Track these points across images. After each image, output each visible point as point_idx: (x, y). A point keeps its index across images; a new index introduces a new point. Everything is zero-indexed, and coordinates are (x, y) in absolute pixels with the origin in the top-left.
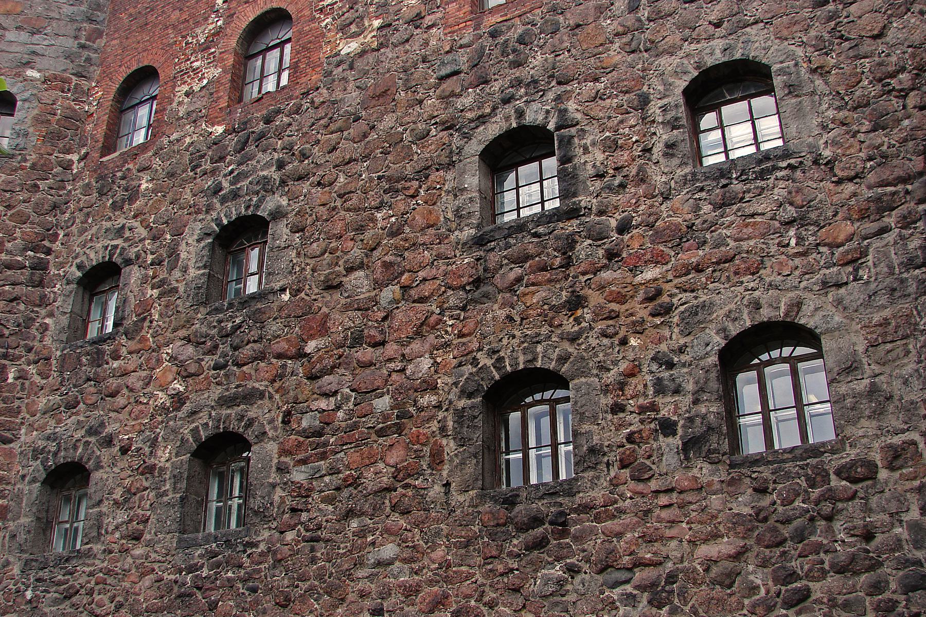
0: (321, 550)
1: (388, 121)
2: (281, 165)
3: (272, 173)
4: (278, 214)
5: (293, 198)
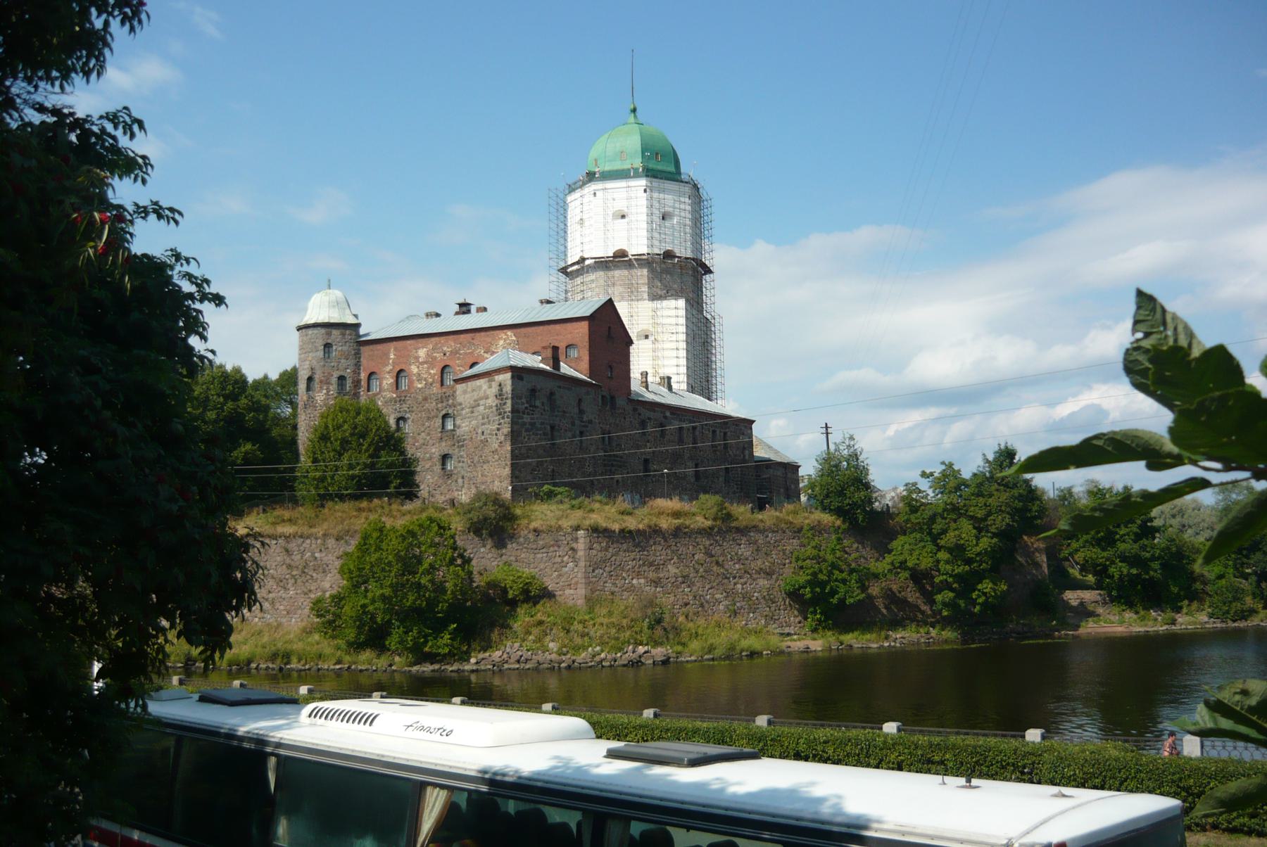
4: (409, 418)
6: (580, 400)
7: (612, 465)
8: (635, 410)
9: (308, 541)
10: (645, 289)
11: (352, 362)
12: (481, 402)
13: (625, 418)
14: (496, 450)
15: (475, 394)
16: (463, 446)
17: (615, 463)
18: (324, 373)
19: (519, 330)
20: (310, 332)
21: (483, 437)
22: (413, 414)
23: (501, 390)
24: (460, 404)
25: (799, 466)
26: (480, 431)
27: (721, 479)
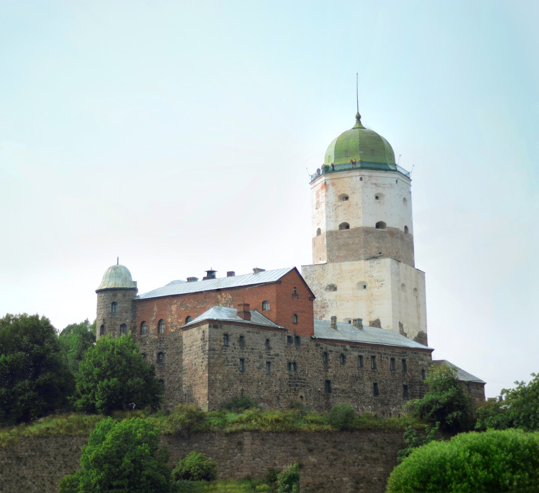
0: (172, 394)
1: (177, 344)
2: (165, 346)
3: (164, 347)
4: (165, 353)
5: (167, 351)
6: (268, 341)
7: (297, 385)
8: (317, 345)
9: (75, 439)
10: (361, 251)
11: (129, 315)
12: (195, 343)
13: (308, 352)
15: (192, 337)
16: (185, 373)
17: (299, 384)
18: (111, 323)
19: (234, 291)
22: (168, 350)
23: (204, 336)
25: (484, 384)
27: (399, 394)
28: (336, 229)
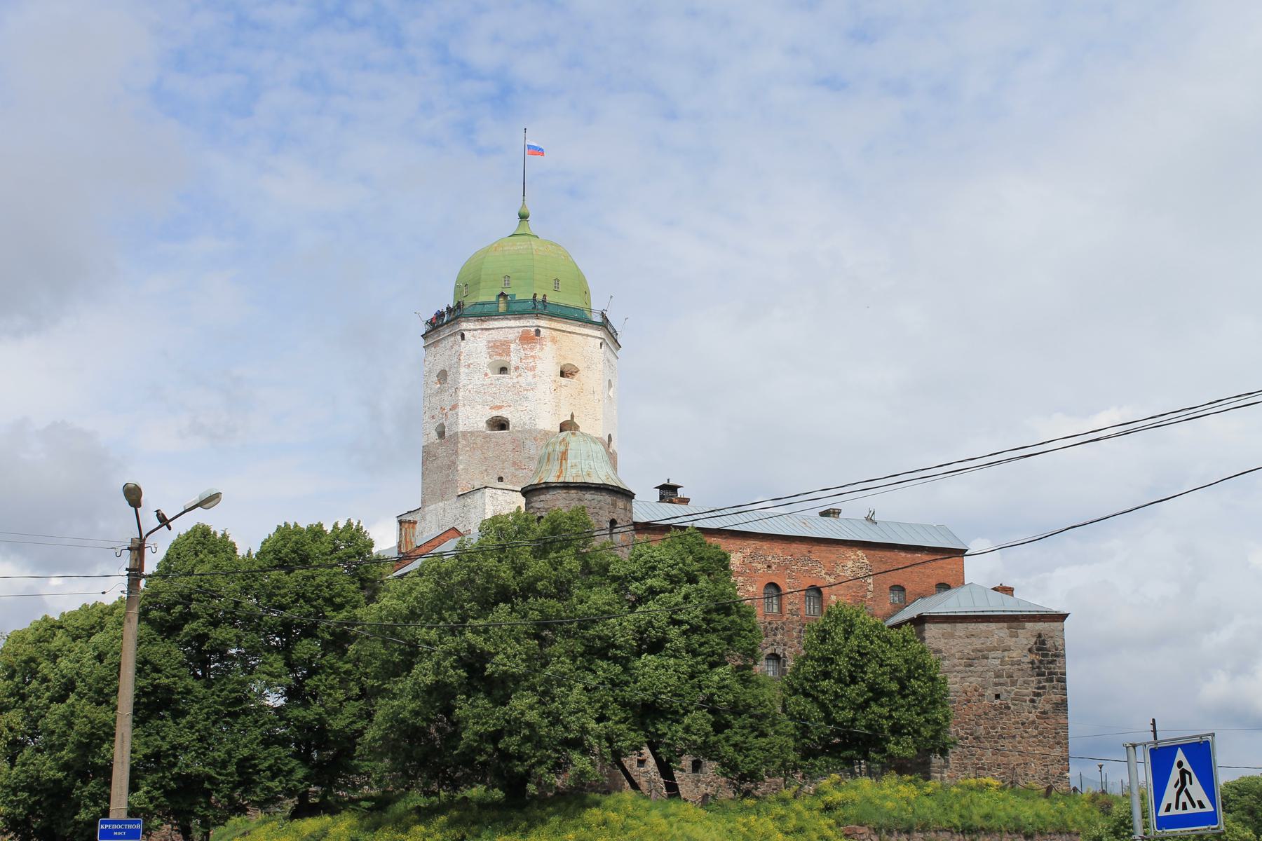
12: (992, 654)
14: (1033, 722)
20: (588, 496)
21: (998, 702)
24: (938, 651)
26: (990, 693)
28: (553, 430)
